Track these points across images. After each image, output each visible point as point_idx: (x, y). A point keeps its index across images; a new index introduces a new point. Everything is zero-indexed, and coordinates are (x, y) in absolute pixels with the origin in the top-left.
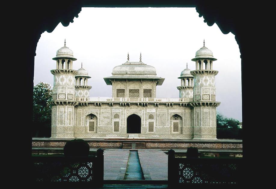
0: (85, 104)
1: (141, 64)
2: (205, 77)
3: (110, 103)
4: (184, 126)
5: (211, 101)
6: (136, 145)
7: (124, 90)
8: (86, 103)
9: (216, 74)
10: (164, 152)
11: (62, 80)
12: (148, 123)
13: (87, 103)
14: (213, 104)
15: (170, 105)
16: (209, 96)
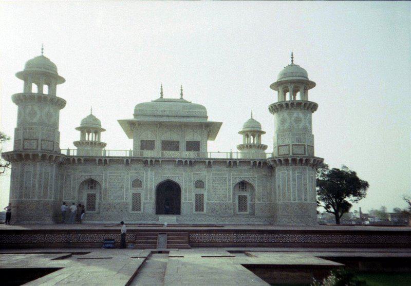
0: (79, 160)
1: (181, 100)
2: (295, 115)
3: (125, 160)
4: (257, 202)
5: (307, 155)
6: (168, 243)
7: (154, 141)
8: (80, 159)
9: (315, 110)
10: (244, 265)
11: (33, 114)
12: (193, 195)
13: (82, 159)
14: (312, 162)
15: (232, 164)
16: (303, 147)
